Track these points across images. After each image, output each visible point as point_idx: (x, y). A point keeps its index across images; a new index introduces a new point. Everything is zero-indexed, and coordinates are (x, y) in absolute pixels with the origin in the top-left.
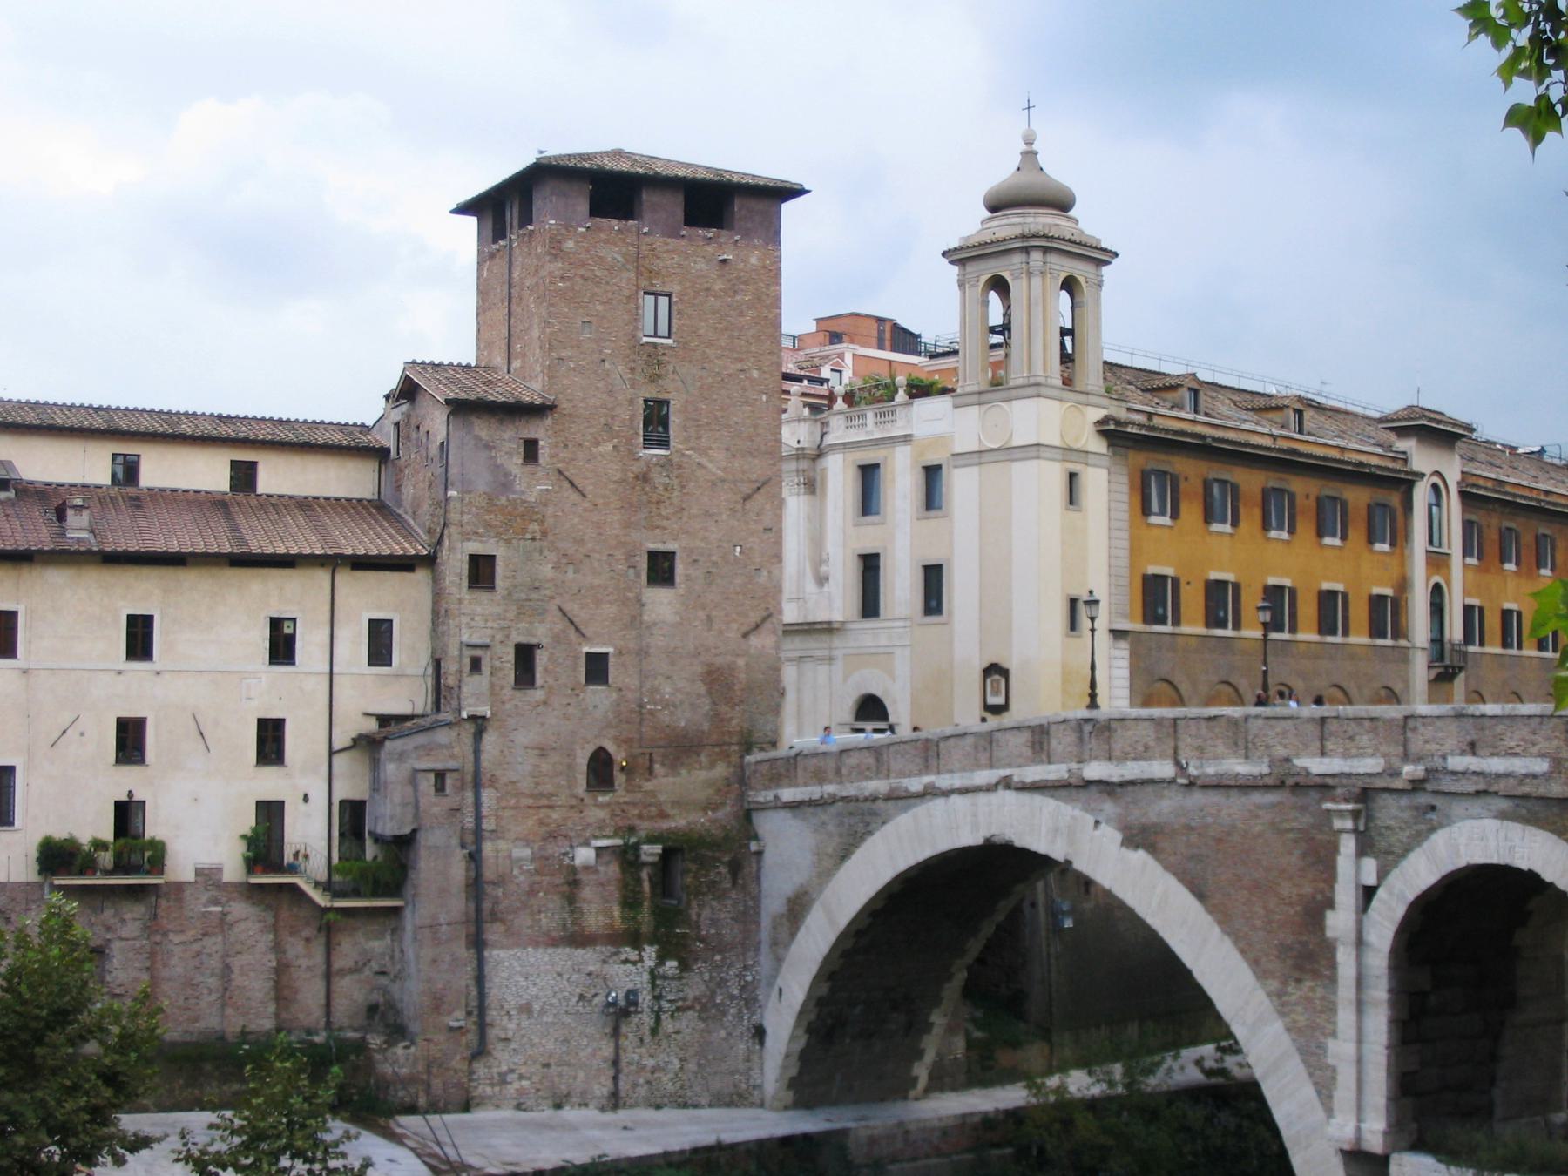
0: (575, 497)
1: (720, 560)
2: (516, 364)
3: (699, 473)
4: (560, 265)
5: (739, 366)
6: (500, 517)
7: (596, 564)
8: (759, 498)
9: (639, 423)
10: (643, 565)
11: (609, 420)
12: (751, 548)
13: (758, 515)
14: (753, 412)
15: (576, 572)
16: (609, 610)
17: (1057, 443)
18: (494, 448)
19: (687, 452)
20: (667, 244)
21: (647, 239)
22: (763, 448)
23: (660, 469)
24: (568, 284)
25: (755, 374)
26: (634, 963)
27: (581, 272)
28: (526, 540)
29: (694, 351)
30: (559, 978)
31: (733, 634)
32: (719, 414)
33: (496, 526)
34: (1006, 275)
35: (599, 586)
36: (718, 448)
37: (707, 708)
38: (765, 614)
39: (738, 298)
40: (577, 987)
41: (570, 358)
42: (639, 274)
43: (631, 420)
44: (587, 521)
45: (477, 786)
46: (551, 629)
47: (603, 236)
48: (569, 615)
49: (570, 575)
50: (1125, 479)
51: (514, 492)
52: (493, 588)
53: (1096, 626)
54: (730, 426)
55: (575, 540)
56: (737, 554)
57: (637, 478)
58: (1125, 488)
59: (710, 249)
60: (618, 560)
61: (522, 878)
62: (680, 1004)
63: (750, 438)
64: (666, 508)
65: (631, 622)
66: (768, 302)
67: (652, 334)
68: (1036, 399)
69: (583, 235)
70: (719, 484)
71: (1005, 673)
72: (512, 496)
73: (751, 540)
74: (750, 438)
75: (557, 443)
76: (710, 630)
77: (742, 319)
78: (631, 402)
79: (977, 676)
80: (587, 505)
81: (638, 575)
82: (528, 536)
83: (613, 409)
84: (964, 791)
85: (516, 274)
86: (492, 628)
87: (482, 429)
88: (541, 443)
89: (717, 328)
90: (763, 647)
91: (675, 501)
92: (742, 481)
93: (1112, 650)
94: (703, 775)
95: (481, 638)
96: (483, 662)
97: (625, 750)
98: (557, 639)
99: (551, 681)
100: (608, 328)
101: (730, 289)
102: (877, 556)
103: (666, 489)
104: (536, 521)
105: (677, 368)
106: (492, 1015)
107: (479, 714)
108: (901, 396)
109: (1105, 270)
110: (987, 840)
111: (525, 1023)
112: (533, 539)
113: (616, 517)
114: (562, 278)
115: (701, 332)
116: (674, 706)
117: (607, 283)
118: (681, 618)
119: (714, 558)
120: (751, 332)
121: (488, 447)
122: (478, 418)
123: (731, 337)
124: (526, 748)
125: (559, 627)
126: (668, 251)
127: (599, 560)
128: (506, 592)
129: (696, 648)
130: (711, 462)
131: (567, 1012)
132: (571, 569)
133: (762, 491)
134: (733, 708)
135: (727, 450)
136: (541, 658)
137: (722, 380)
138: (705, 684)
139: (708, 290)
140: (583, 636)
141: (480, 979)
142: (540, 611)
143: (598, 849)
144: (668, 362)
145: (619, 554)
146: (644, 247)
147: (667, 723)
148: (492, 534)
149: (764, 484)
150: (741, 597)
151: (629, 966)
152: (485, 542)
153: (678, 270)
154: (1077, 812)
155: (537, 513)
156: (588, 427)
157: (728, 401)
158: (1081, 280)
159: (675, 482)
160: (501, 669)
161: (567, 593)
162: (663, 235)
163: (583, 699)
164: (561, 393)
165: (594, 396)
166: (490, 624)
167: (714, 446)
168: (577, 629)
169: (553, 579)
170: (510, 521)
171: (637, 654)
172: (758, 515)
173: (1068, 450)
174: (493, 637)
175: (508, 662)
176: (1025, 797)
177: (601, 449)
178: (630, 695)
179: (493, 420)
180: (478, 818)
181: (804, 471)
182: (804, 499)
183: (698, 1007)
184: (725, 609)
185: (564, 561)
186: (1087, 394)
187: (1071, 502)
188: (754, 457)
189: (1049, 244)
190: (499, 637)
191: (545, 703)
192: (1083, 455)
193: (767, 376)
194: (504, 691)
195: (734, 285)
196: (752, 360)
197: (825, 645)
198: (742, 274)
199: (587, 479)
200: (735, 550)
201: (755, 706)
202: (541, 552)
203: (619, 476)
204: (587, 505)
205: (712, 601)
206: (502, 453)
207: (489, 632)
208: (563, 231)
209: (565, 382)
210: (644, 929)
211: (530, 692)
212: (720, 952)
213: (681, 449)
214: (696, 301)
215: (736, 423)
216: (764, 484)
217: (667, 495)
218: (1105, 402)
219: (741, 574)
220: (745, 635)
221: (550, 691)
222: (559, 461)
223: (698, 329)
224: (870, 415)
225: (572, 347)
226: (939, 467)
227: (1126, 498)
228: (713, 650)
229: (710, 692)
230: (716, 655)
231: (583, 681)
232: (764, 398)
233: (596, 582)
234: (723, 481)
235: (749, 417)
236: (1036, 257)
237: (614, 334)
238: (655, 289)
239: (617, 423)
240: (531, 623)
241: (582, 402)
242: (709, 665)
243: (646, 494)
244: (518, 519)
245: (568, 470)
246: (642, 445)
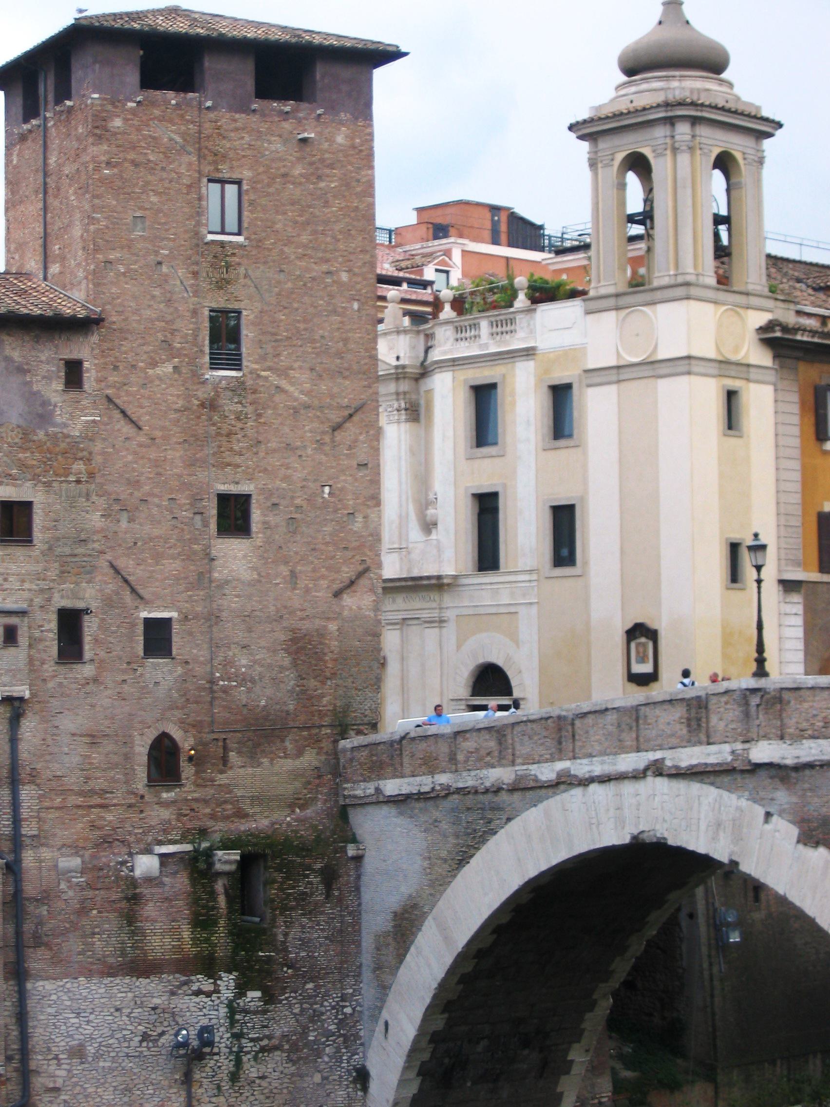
0: (127, 429)
1: (305, 504)
2: (55, 269)
3: (278, 398)
4: (106, 148)
5: (325, 267)
6: (37, 455)
7: (155, 511)
8: (351, 429)
9: (203, 341)
10: (213, 512)
11: (169, 335)
12: (342, 489)
13: (350, 448)
14: (342, 322)
15: (131, 520)
16: (173, 566)
17: (712, 354)
18: (29, 371)
19: (263, 373)
20: (235, 121)
21: (212, 115)
22: (355, 367)
23: (230, 393)
24: (116, 170)
25: (344, 277)
26: (208, 995)
27: (131, 156)
28: (69, 482)
29: (270, 250)
30: (117, 1014)
31: (323, 593)
32: (302, 326)
33: (33, 466)
34: (647, 152)
35: (157, 537)
36: (301, 368)
37: (292, 683)
38: (360, 568)
39: (322, 185)
40: (140, 1024)
41: (119, 261)
42: (201, 157)
43: (195, 336)
44: (142, 458)
45: (14, 781)
46: (101, 590)
47: (157, 112)
48: (123, 573)
49: (124, 524)
50: (795, 398)
51: (55, 425)
52: (31, 541)
53: (762, 576)
54: (313, 341)
55: (129, 482)
56: (326, 496)
57: (202, 405)
58: (796, 409)
59: (287, 125)
60: (181, 506)
61: (71, 893)
62: (265, 1042)
63: (339, 355)
64: (239, 441)
65: (199, 579)
66: (359, 189)
67: (219, 229)
68: (685, 302)
69: (133, 111)
70: (302, 412)
71: (653, 635)
72: (51, 430)
73: (343, 478)
74: (339, 355)
75: (106, 364)
76: (294, 589)
77: (326, 210)
78: (195, 313)
79: (619, 638)
80: (142, 439)
81: (206, 524)
82: (72, 478)
83: (171, 322)
84: (605, 779)
85: (52, 160)
86: (30, 590)
87: (13, 349)
88: (86, 365)
89: (296, 222)
90: (360, 608)
91: (251, 433)
92: (330, 407)
93: (782, 604)
94: (288, 764)
95: (16, 602)
96: (20, 632)
97: (194, 736)
98: (109, 602)
99: (102, 654)
100: (165, 223)
101: (312, 174)
102: (494, 496)
103: (238, 419)
104: (81, 459)
105: (250, 272)
106: (37, 1060)
107: (15, 694)
108: (521, 301)
109: (767, 143)
110: (635, 838)
111: (78, 1069)
112: (78, 482)
113: (176, 454)
114: (108, 164)
115: (279, 226)
116: (253, 681)
117: (163, 169)
118: (259, 574)
119: (298, 501)
120: (337, 227)
121: (21, 370)
122: (9, 335)
123: (314, 232)
124: (74, 735)
125: (110, 588)
126: (237, 129)
127: (158, 506)
128: (46, 546)
129: (278, 611)
130: (292, 384)
131: (127, 1056)
132: (124, 516)
133: (356, 418)
134: (323, 683)
135: (312, 369)
136: (90, 627)
137: (305, 285)
138: (289, 653)
139: (285, 175)
140: (141, 598)
141: (22, 1017)
142: (88, 568)
143: (162, 856)
144: (239, 264)
145: (183, 499)
146: (207, 125)
147: (244, 703)
148: (29, 477)
149: (357, 410)
150: (331, 548)
151: (203, 998)
152: (21, 486)
153: (249, 153)
154: (744, 803)
155: (82, 450)
156: (144, 345)
157: (311, 310)
158: (738, 156)
159: (250, 409)
160: (41, 640)
161: (120, 545)
162: (232, 109)
163: (141, 675)
164: (109, 303)
165: (149, 306)
166: (27, 586)
167: (296, 365)
168: (133, 591)
169: (102, 530)
170: (50, 459)
171: (208, 620)
172: (350, 448)
173: (725, 363)
174: (32, 600)
176: (681, 786)
177: (158, 371)
178: (199, 670)
179: (27, 338)
180: (16, 821)
181: (405, 393)
182: (405, 427)
183: (286, 1047)
184: (312, 563)
185: (117, 507)
186: (747, 294)
187: (730, 427)
188: (345, 378)
189: (699, 114)
190: (38, 601)
191: (95, 680)
192: (744, 369)
193: (359, 279)
194: (45, 666)
195: (317, 169)
196: (340, 260)
197: (434, 605)
198: (327, 156)
199: (142, 407)
200: (323, 492)
201: (350, 680)
202: (88, 496)
203: (181, 403)
204: (142, 439)
205: (296, 553)
206: (39, 378)
207: (26, 595)
208: (110, 107)
209: (114, 290)
210: (220, 953)
211: (78, 667)
212: (312, 980)
213: (257, 370)
214: (271, 190)
215: (322, 337)
216: (357, 410)
217: (239, 425)
218: (770, 304)
219: (332, 520)
220: (337, 594)
221: (101, 665)
222: (108, 387)
223: (274, 223)
224: (484, 324)
225: (122, 248)
226: (568, 387)
227: (796, 420)
228: (298, 613)
229: (295, 664)
230: (302, 619)
231: (141, 653)
232: (356, 306)
233: (156, 532)
234: (307, 407)
235: (339, 329)
236: (683, 129)
237: (173, 230)
238: (220, 175)
239: (178, 339)
240: (77, 584)
241: (134, 313)
242: (293, 631)
243: (214, 424)
244: (59, 457)
245: (119, 398)
246: (208, 365)
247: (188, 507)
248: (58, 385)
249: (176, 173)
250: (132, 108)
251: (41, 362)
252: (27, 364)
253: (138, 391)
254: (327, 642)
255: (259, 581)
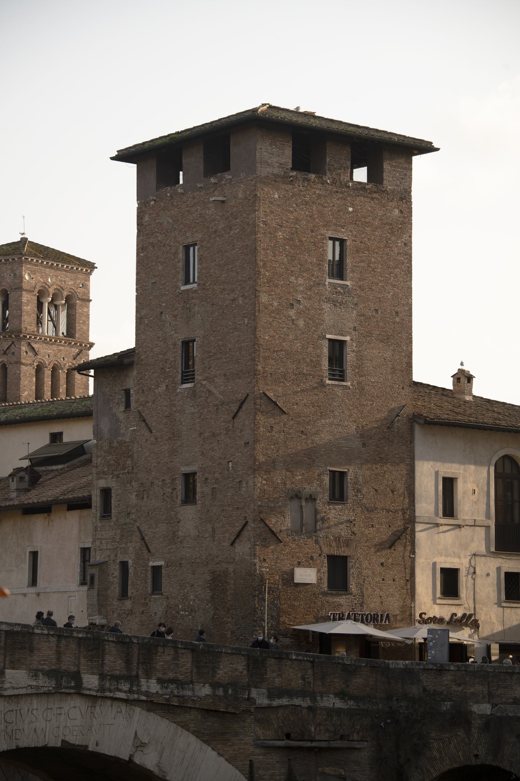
0: (147, 433)
76: (214, 541)
90: (244, 554)
135: (225, 375)
137: (223, 312)
139: (215, 232)
165: (157, 344)
174: (110, 556)
175: (116, 577)
220: (232, 544)
246: (180, 381)
247: (169, 485)
248: (122, 408)
249: (169, 246)
250: (153, 206)
251: (116, 393)
252: (111, 396)
253: (151, 405)
254: (228, 580)
255: (199, 536)
